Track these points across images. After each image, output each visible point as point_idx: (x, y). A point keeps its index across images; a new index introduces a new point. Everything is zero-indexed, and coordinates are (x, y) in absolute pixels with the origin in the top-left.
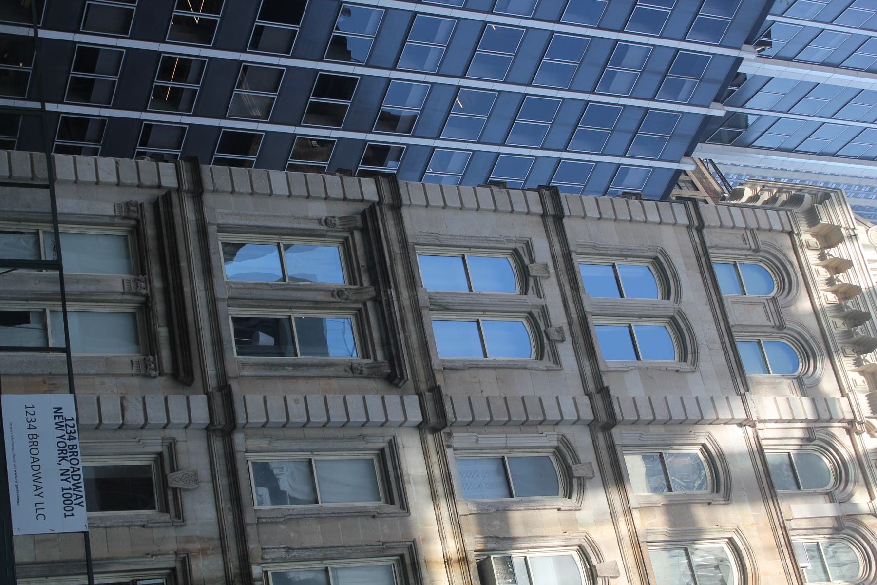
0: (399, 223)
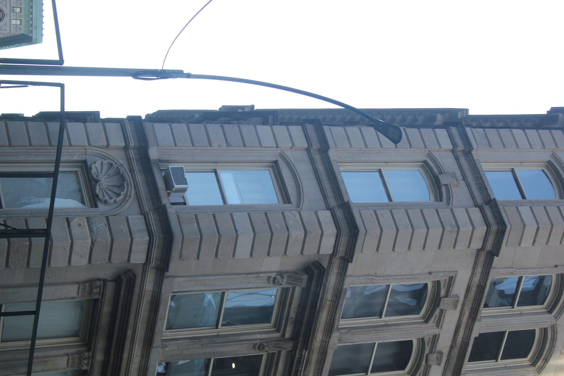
0: (342, 274)
